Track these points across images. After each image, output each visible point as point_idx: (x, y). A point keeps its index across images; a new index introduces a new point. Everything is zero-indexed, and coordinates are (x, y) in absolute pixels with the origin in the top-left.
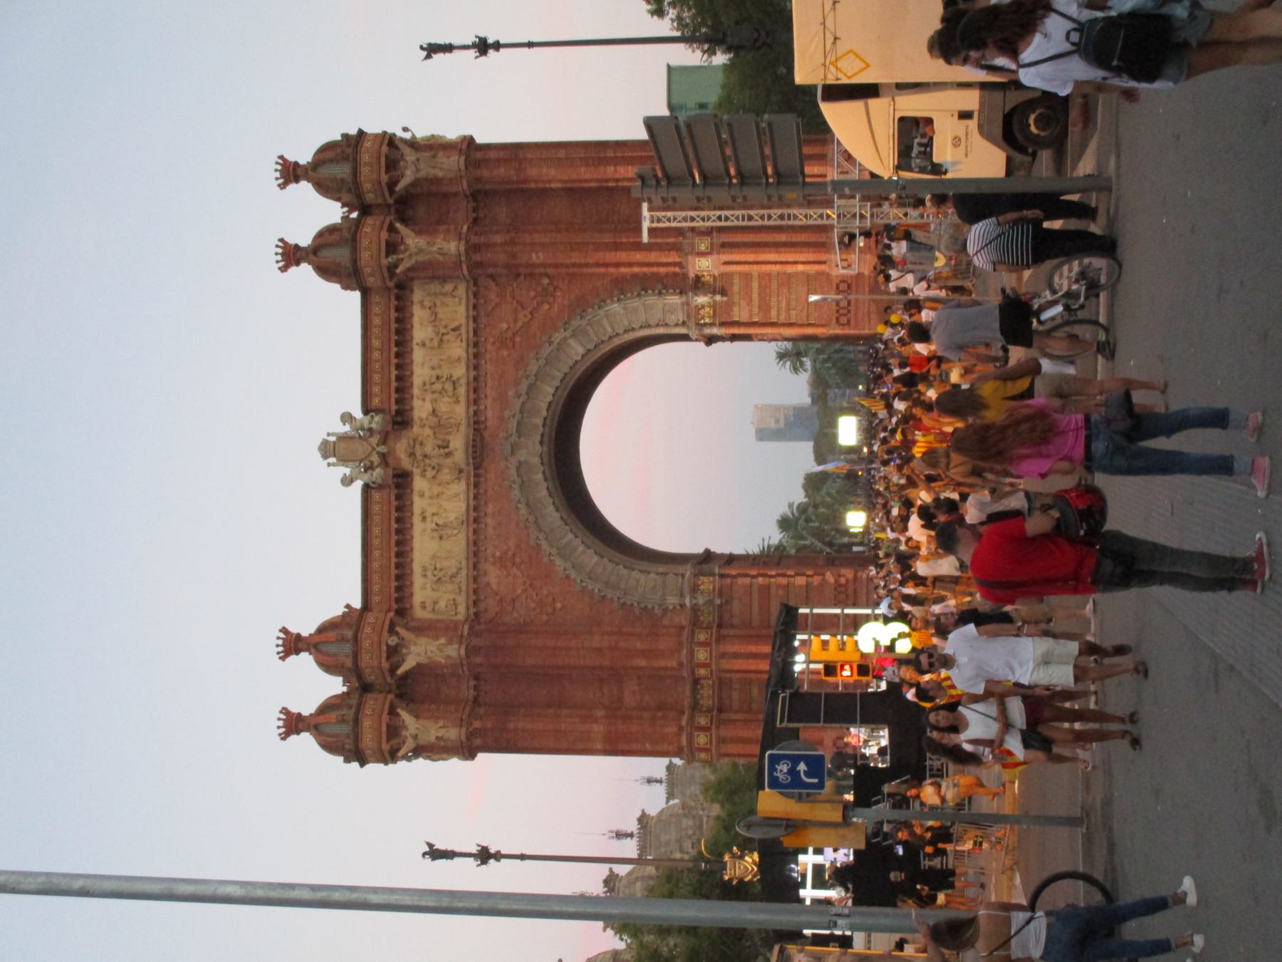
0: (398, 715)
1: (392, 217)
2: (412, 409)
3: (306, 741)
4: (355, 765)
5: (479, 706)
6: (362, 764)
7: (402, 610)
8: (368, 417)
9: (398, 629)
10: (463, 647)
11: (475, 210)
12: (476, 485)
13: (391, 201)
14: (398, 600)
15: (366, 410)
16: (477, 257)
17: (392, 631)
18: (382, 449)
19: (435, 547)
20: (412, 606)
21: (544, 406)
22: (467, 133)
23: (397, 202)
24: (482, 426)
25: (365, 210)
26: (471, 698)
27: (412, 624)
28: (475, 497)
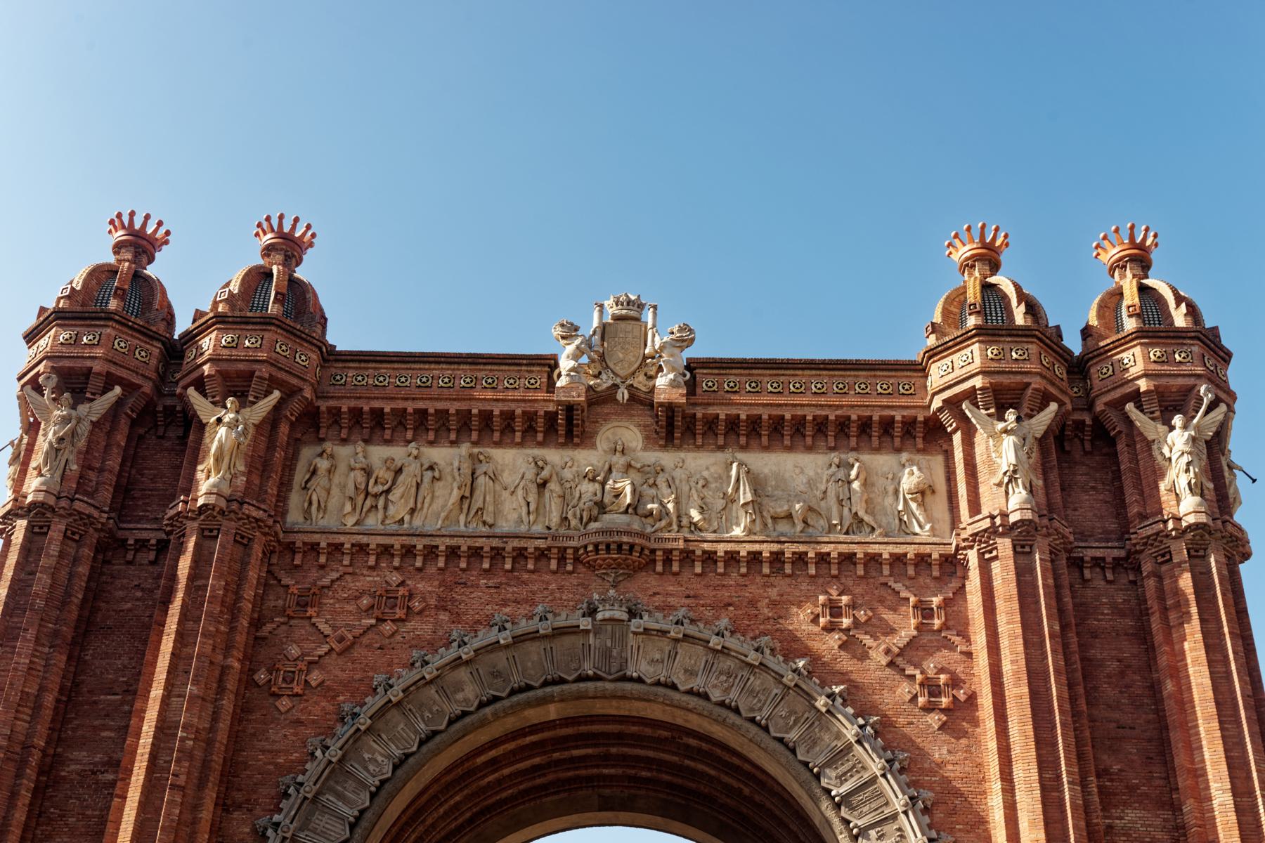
0: (107, 389)
1: (1069, 407)
2: (698, 448)
5: (100, 548)
8: (682, 370)
9: (277, 394)
10: (223, 503)
11: (1098, 562)
12: (542, 555)
13: (1099, 406)
14: (335, 413)
15: (691, 366)
16: (1004, 546)
17: (273, 383)
18: (623, 395)
19: (427, 490)
20: (322, 440)
21: (697, 683)
22: (1254, 545)
23: (1096, 419)
24: (659, 568)
25: (1079, 368)
26: (120, 534)
27: (284, 429)
28: (520, 554)
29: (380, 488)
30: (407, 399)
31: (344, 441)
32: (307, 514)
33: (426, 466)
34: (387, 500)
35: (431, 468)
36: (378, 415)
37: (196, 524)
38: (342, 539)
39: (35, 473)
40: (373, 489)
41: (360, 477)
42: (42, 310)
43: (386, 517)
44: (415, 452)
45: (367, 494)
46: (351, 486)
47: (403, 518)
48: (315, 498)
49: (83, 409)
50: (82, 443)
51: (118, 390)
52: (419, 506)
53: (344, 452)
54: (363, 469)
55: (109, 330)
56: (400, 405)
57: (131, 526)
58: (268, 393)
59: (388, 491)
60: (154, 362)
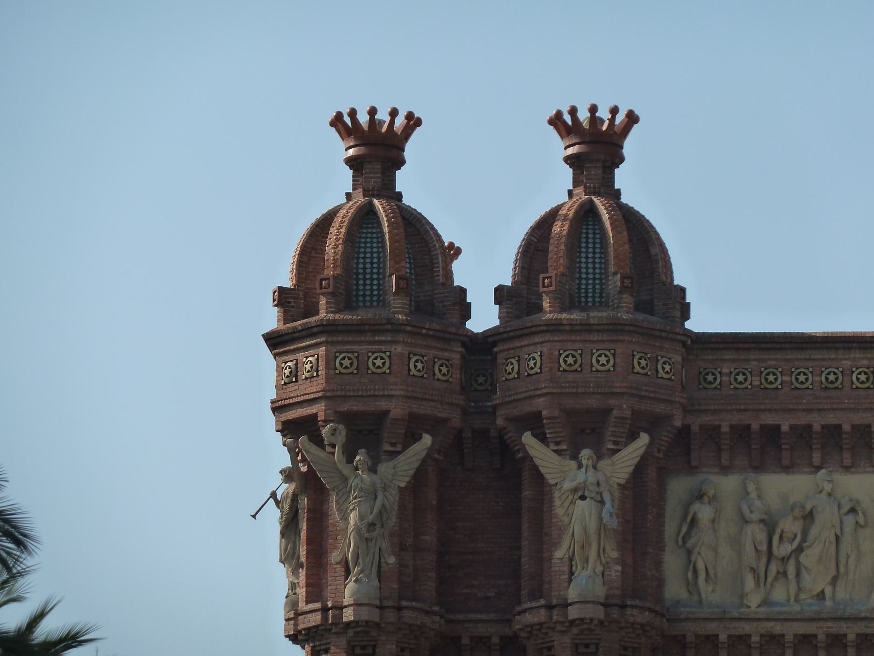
0: (412, 437)
3: (332, 185)
4: (271, 319)
6: (274, 341)
7: (683, 448)
9: (644, 438)
10: (599, 613)
14: (712, 432)
27: (651, 473)
29: (786, 549)
30: (809, 411)
31: (725, 470)
32: (692, 586)
33: (846, 509)
34: (798, 564)
35: (853, 510)
36: (772, 433)
37: (567, 640)
38: (746, 628)
39: (340, 570)
40: (782, 550)
41: (761, 536)
42: (281, 291)
43: (800, 589)
44: (828, 487)
45: (770, 554)
46: (749, 548)
47: (823, 592)
48: (701, 566)
49: (385, 468)
50: (392, 521)
51: (427, 440)
52: (842, 569)
53: (727, 484)
54: (762, 521)
55: (399, 349)
56: (803, 419)
57: (461, 617)
58: (633, 436)
59: (800, 549)
60: (457, 375)
